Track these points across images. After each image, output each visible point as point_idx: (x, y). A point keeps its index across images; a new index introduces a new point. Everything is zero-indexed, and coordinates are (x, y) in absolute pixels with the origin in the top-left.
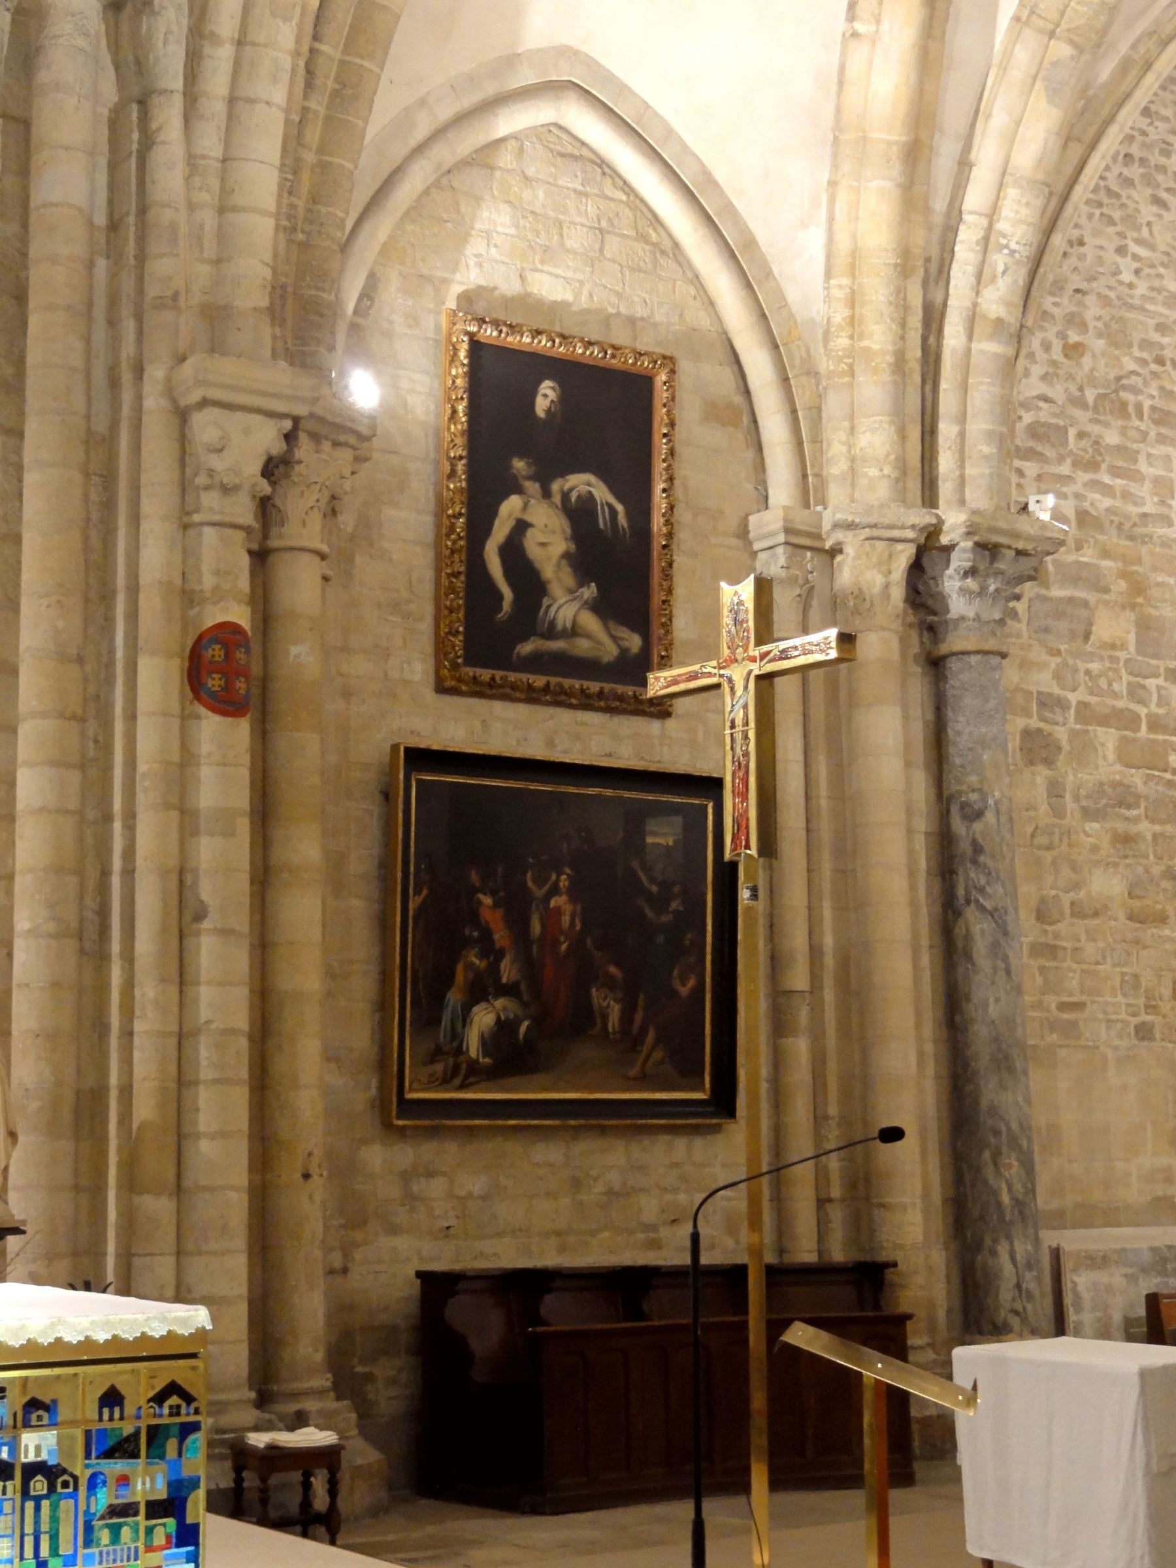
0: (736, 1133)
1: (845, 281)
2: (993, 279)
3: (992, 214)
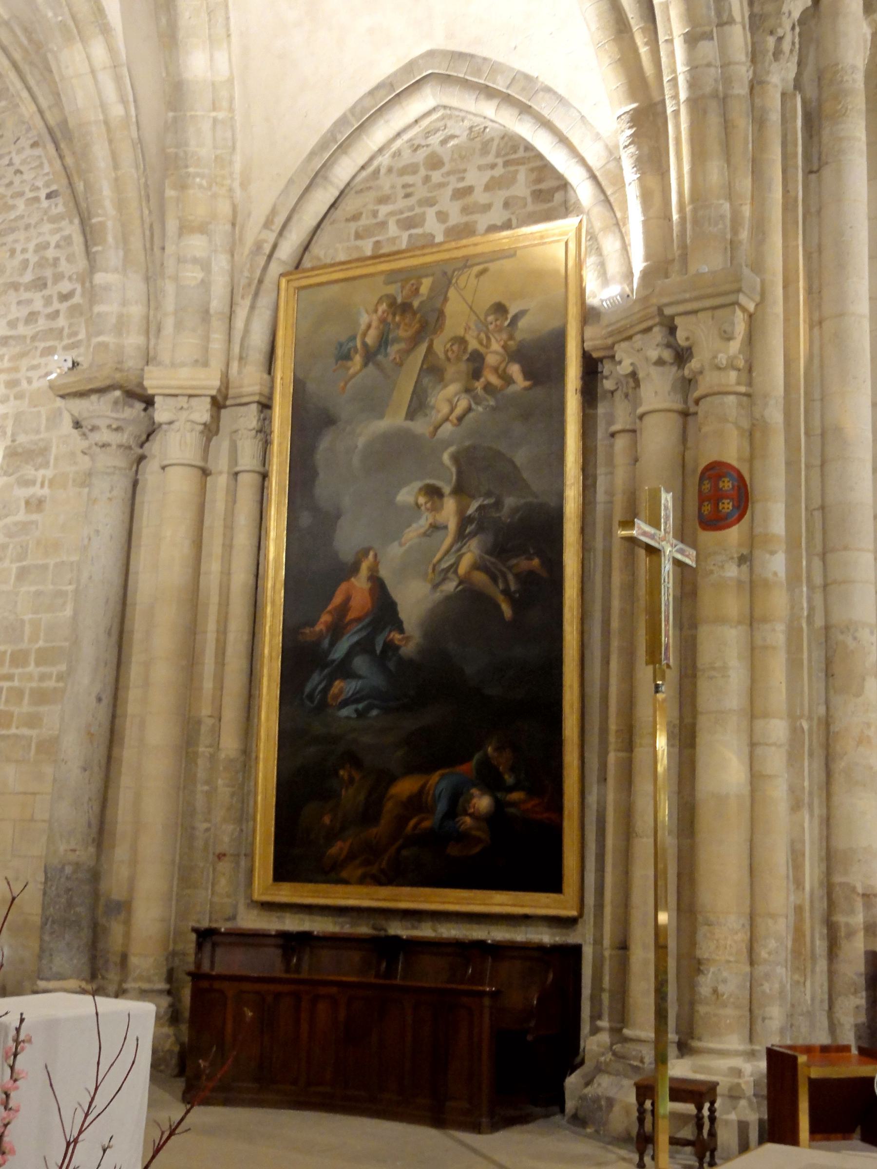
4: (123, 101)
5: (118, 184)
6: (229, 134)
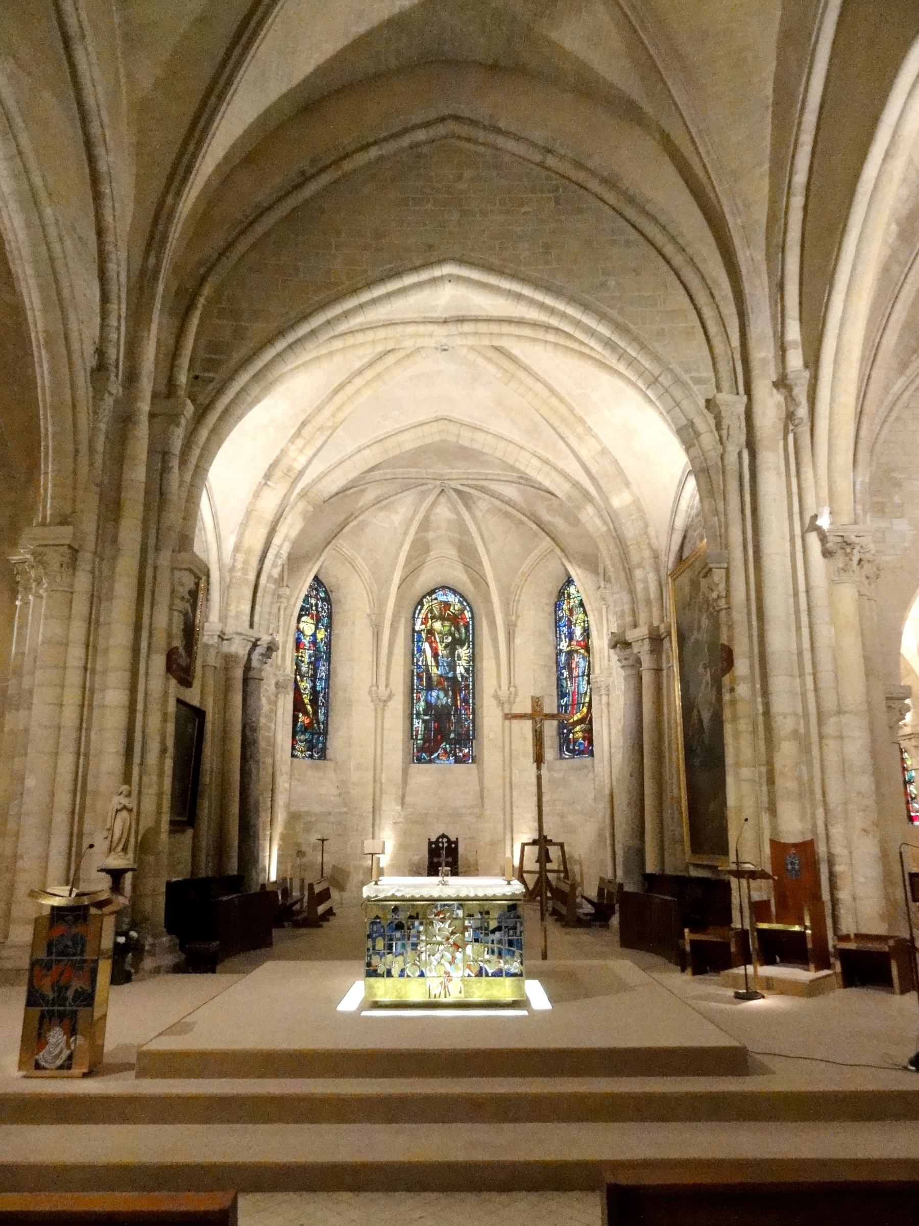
0: (190, 832)
1: (243, 556)
2: (276, 566)
3: (280, 547)
4: (605, 523)
5: (611, 558)
6: (640, 523)
